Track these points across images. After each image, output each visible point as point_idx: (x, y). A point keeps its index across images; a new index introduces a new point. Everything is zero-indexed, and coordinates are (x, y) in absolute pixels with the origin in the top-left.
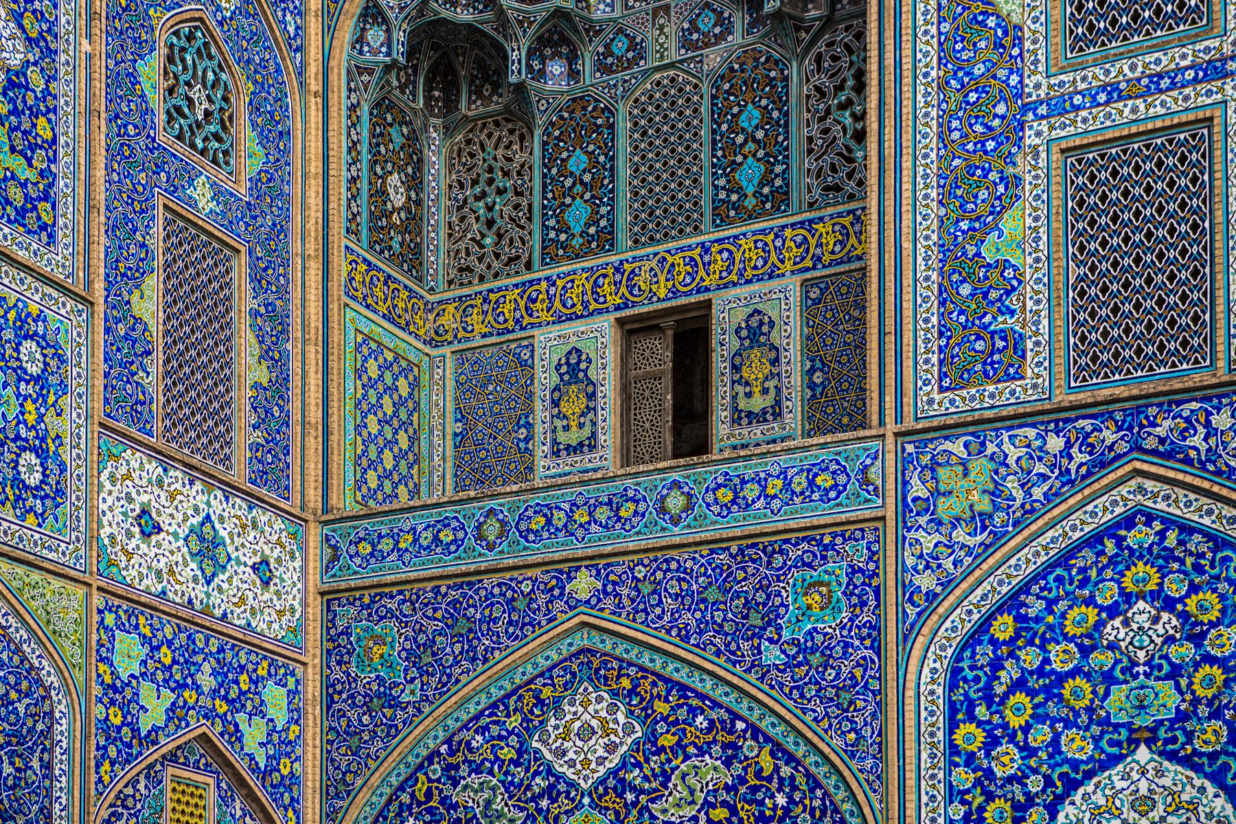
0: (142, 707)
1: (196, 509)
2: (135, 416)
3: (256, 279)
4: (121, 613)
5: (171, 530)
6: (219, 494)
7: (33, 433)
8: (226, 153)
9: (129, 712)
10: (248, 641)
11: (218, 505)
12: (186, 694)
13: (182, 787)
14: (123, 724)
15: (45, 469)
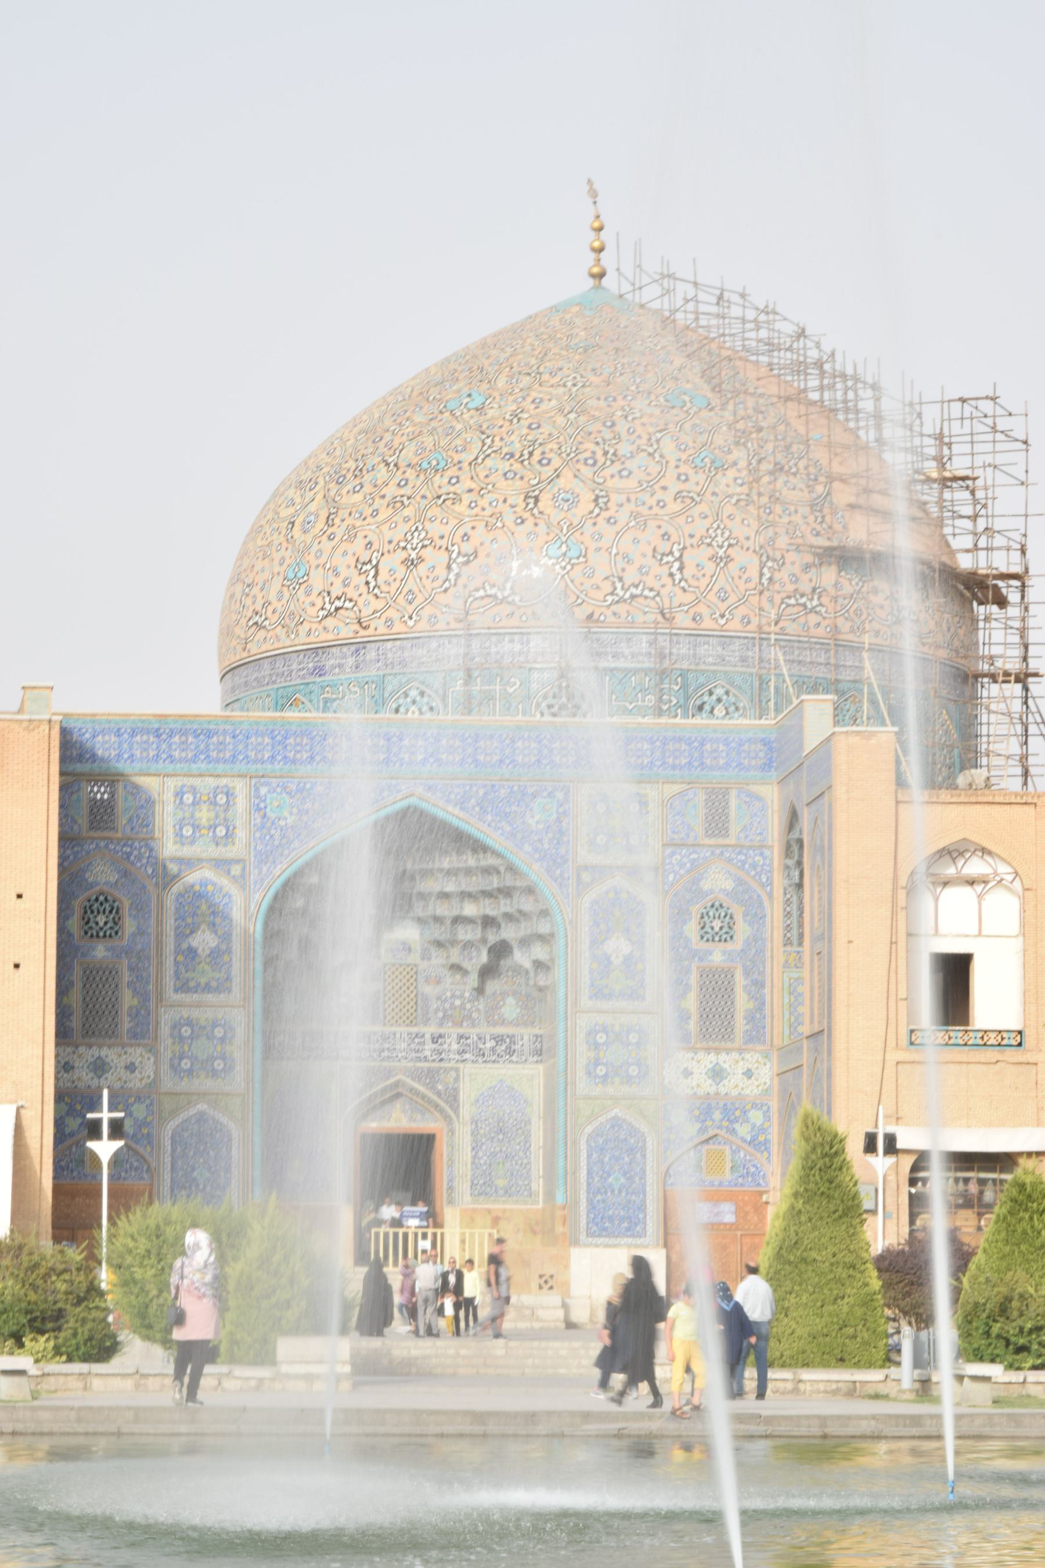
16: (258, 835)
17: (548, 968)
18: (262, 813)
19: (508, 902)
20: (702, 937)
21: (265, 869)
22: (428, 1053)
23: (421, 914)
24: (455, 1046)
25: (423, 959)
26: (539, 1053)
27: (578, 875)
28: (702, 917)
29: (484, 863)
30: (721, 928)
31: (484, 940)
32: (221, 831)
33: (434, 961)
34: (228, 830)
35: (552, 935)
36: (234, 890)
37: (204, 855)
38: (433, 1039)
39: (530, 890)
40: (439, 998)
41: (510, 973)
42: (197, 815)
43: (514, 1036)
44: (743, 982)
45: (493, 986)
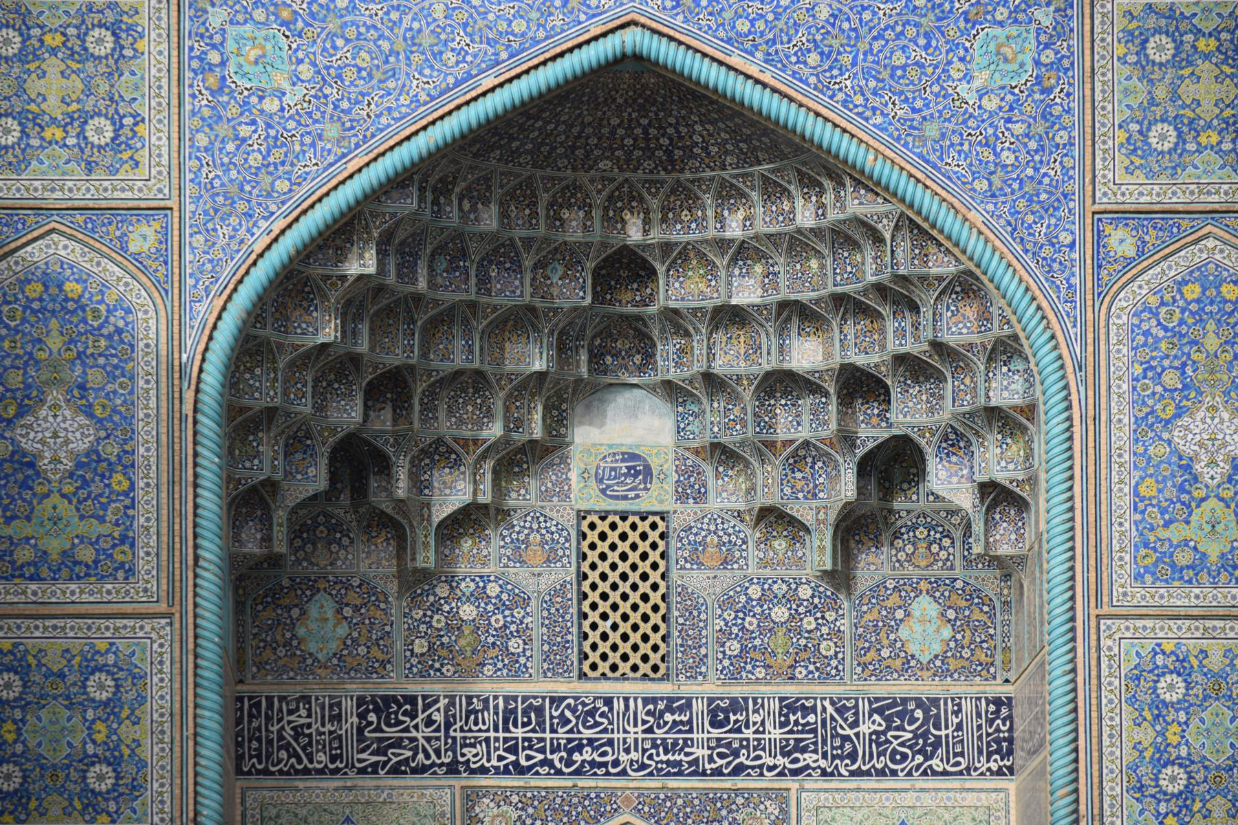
16: (202, 140)
17: (1021, 505)
18: (212, 81)
19: (907, 323)
21: (223, 231)
22: (700, 752)
23: (674, 374)
24: (775, 733)
25: (682, 497)
26: (1004, 747)
27: (1099, 235)
29: (834, 215)
31: (847, 440)
32: (100, 131)
33: (714, 503)
34: (118, 128)
35: (1030, 410)
36: (138, 295)
37: (54, 198)
38: (713, 713)
39: (967, 286)
40: (727, 602)
41: (921, 533)
42: (34, 86)
43: (935, 702)
45: (873, 566)
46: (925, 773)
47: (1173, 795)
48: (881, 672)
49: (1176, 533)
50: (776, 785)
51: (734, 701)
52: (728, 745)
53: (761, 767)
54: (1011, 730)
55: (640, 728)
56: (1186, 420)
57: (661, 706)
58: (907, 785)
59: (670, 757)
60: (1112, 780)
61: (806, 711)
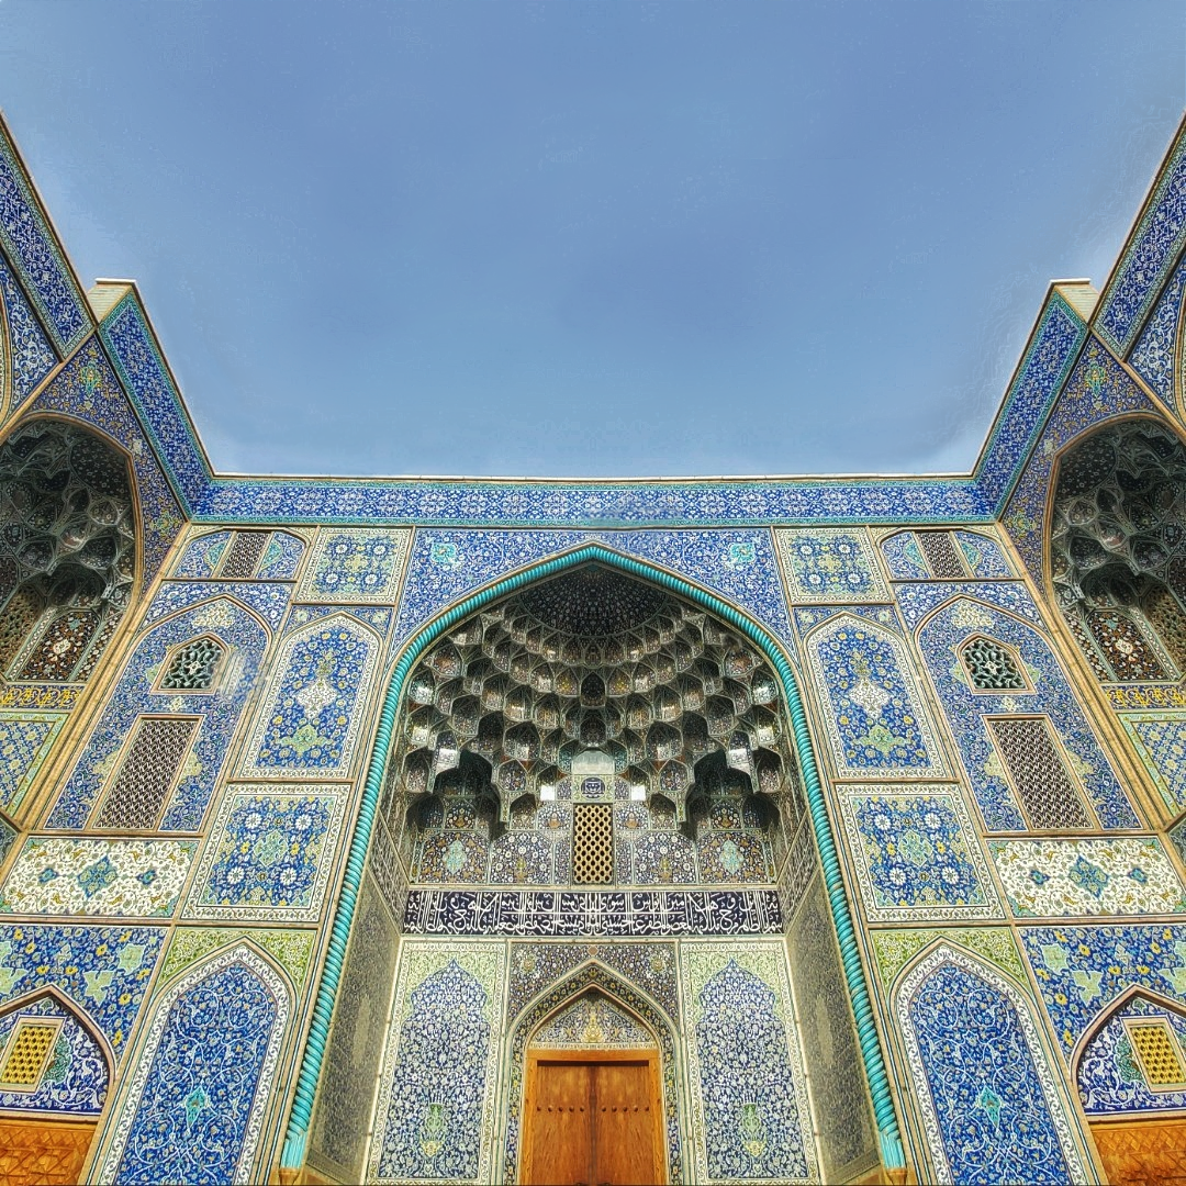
0: (1079, 988)
1: (1070, 857)
2: (1009, 823)
3: (1062, 726)
4: (1040, 934)
5: (1056, 875)
6: (1083, 843)
7: (946, 857)
8: (1017, 681)
9: (1070, 994)
10: (1144, 918)
11: (1084, 849)
12: (1111, 969)
13: (1142, 1031)
14: (1069, 1002)
15: (959, 872)
20: (979, 683)
22: (629, 922)
24: (665, 912)
26: (777, 917)
28: (968, 660)
30: (999, 671)
38: (635, 901)
43: (740, 894)
44: (1063, 738)
46: (740, 933)
47: (901, 887)
48: (712, 879)
49: (863, 742)
50: (667, 940)
51: (644, 894)
52: (643, 919)
53: (659, 930)
54: (779, 908)
55: (600, 909)
56: (854, 689)
57: (610, 897)
58: (732, 939)
59: (615, 925)
60: (863, 877)
61: (679, 900)
